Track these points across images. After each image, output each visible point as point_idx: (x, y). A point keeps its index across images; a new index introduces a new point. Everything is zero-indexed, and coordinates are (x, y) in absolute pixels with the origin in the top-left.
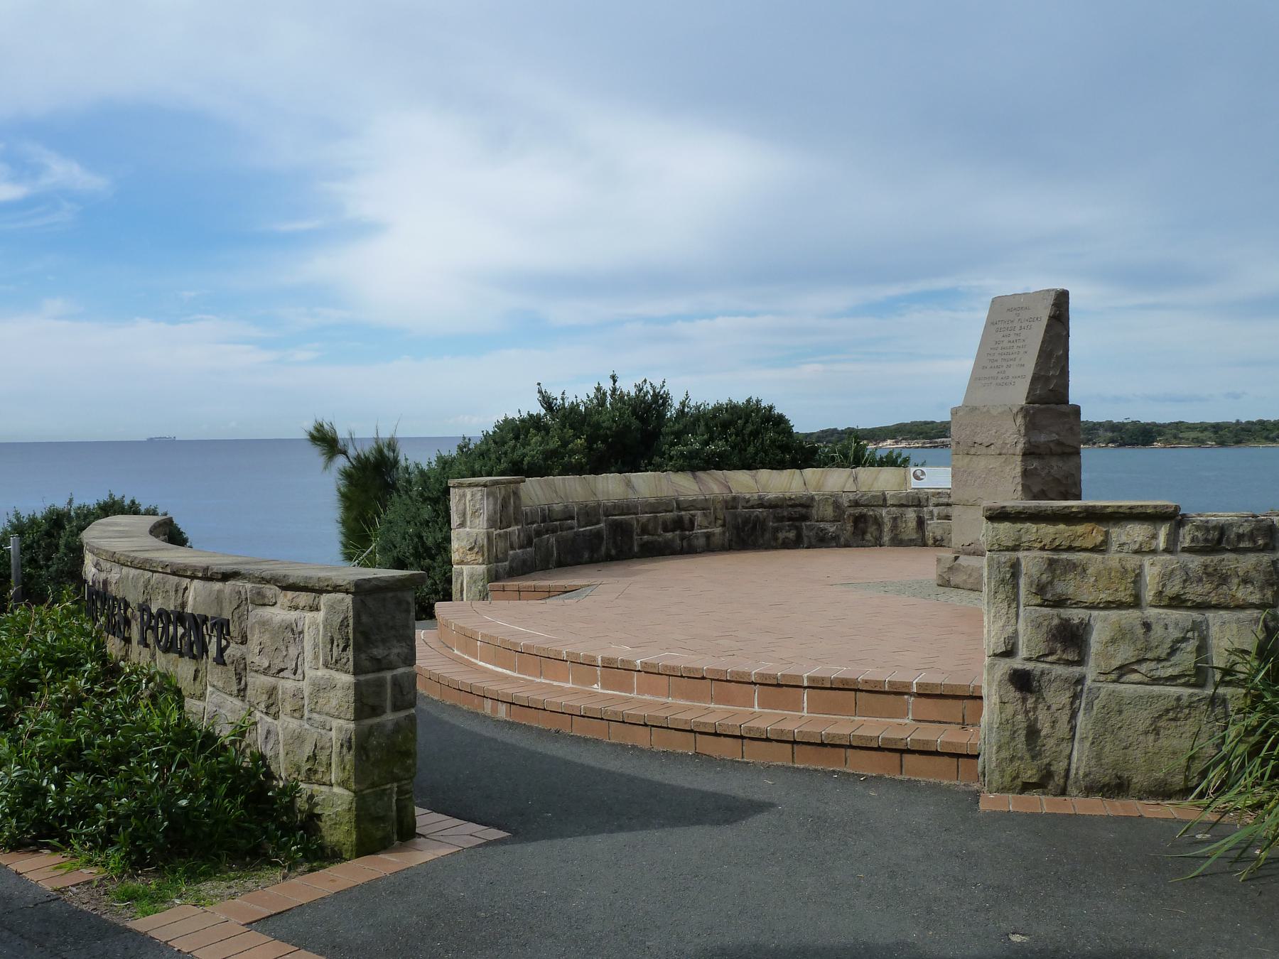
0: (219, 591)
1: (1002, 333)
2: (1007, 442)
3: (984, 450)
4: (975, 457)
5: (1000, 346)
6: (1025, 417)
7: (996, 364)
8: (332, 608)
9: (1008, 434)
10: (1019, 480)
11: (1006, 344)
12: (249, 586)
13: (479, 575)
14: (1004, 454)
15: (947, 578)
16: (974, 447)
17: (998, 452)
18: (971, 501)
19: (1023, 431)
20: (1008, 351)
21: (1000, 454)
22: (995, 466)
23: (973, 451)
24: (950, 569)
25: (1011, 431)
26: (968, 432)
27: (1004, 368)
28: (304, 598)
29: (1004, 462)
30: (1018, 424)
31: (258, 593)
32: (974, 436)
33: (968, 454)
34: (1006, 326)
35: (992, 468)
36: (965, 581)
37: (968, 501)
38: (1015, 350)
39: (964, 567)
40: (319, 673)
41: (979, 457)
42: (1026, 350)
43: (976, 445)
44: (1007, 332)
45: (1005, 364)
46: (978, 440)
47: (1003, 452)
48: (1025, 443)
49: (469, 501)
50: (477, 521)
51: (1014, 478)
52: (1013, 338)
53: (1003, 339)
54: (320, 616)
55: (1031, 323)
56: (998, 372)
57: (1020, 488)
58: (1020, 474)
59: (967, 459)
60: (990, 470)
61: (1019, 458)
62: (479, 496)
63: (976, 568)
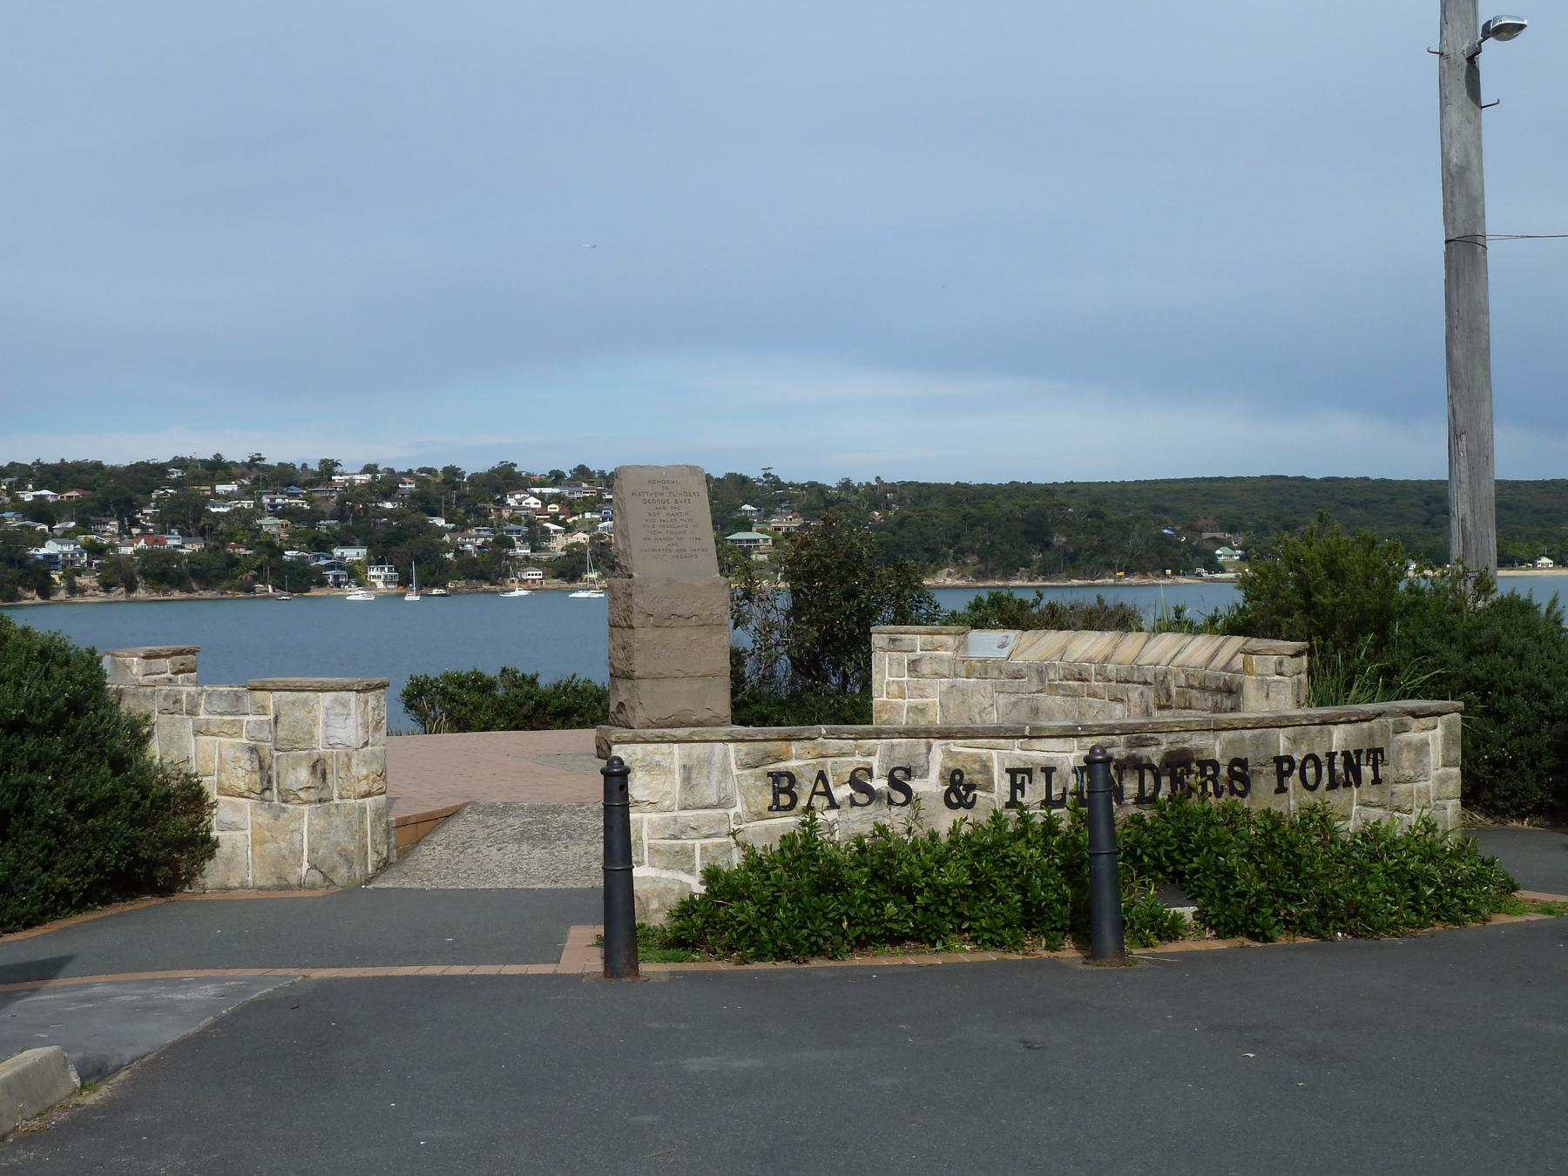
0: (1371, 729)
3: (681, 621)
4: (667, 630)
7: (659, 536)
8: (1448, 726)
11: (663, 516)
12: (1391, 720)
13: (383, 808)
14: (709, 625)
17: (701, 623)
23: (667, 623)
27: (675, 540)
28: (1429, 721)
31: (1402, 724)
40: (1439, 771)
41: (673, 630)
44: (661, 505)
46: (678, 613)
47: (708, 623)
49: (374, 709)
50: (377, 736)
53: (656, 511)
54: (1439, 732)
55: (689, 498)
59: (658, 632)
62: (372, 702)
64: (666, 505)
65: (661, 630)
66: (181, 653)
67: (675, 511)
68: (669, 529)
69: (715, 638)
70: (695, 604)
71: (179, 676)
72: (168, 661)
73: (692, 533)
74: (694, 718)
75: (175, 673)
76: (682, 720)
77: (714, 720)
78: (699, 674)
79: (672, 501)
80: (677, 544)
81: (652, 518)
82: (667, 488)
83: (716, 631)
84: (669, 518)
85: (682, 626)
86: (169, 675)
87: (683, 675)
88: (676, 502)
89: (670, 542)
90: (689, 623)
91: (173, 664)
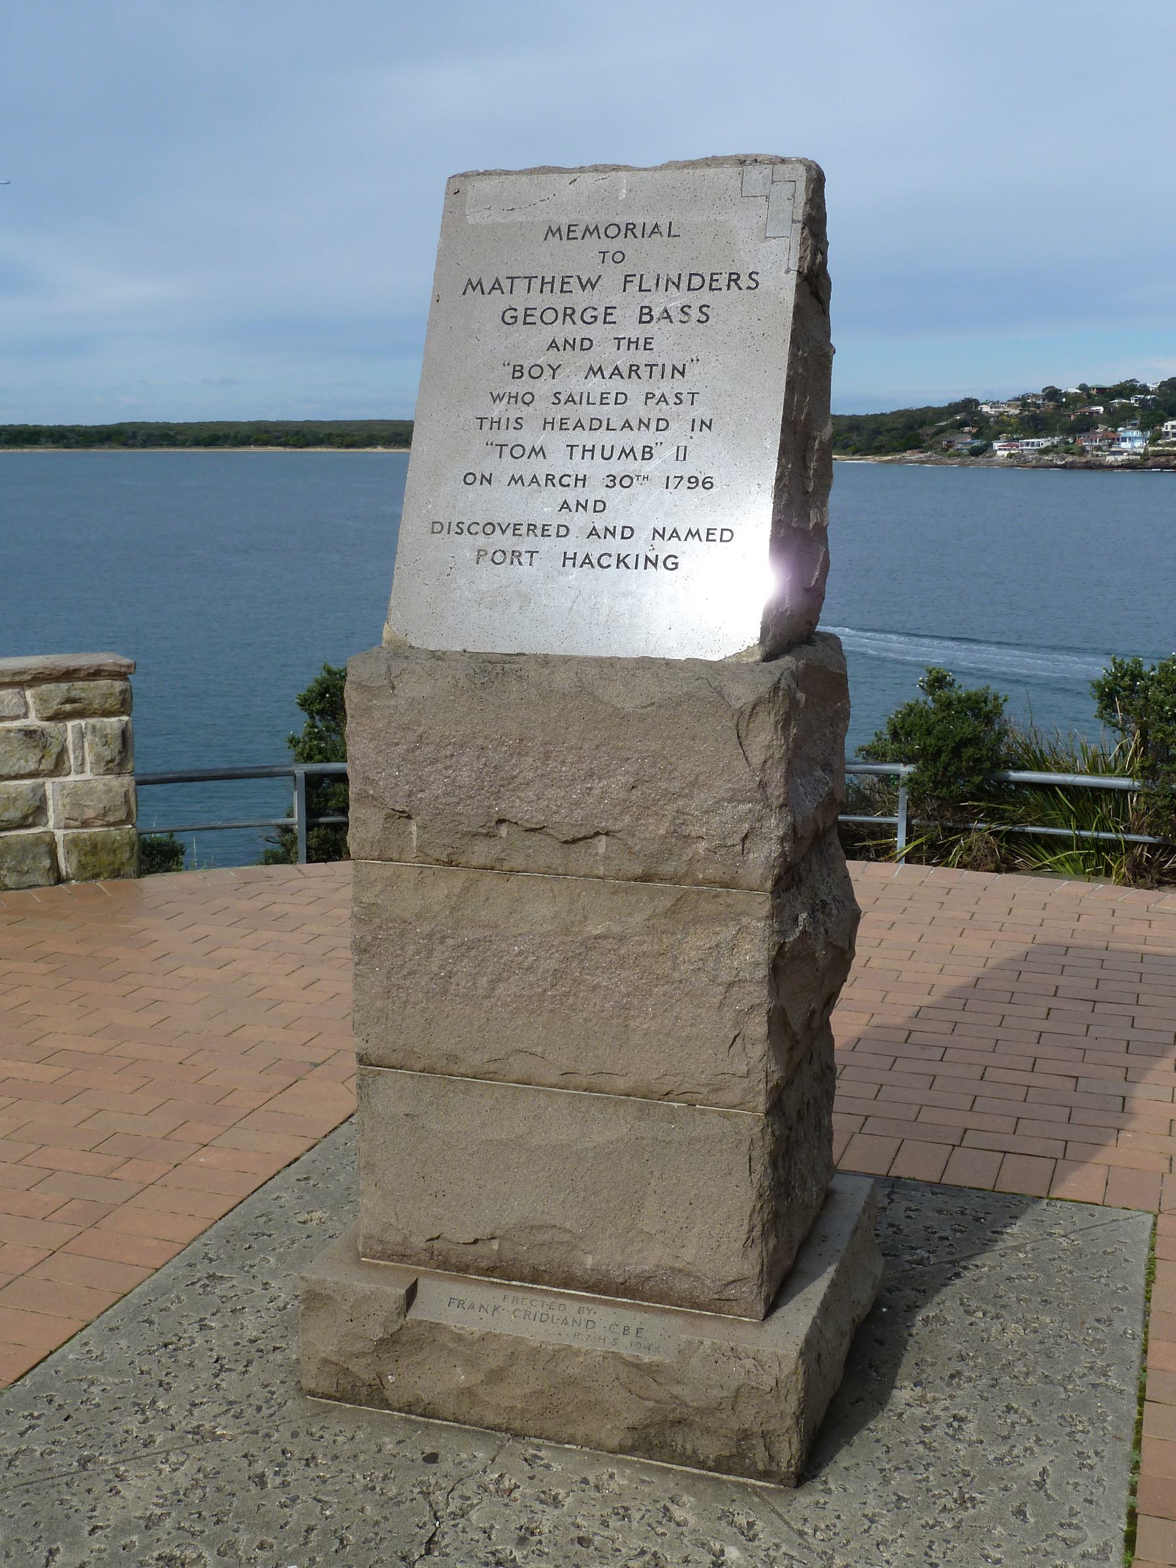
1: (547, 334)
2: (694, 830)
3: (547, 853)
4: (489, 881)
5: (544, 387)
6: (785, 723)
9: (703, 798)
10: (758, 995)
14: (675, 879)
15: (367, 1376)
16: (489, 835)
17: (638, 870)
18: (476, 1060)
19: (776, 791)
20: (604, 412)
21: (646, 878)
22: (616, 929)
23: (482, 852)
24: (390, 1343)
25: (722, 788)
26: (465, 776)
29: (670, 913)
30: (757, 758)
32: (497, 795)
33: (450, 863)
34: (560, 302)
35: (604, 937)
36: (468, 1392)
37: (453, 1058)
38: (636, 409)
39: (459, 1339)
41: (514, 882)
42: (701, 411)
43: (504, 830)
45: (597, 469)
46: (523, 808)
47: (668, 868)
48: (782, 840)
51: (730, 985)
52: (606, 354)
53: (553, 357)
55: (706, 296)
56: (565, 505)
57: (758, 1027)
58: (762, 972)
60: (591, 944)
61: (762, 905)
63: (535, 1352)
64: (597, 331)
65: (457, 881)
66: (69, 675)
67: (624, 359)
68: (583, 438)
69: (696, 943)
70: (599, 786)
71: (70, 724)
72: (28, 693)
73: (682, 454)
74: (589, 1261)
75: (58, 717)
76: (538, 1259)
77: (682, 1285)
78: (621, 1084)
79: (628, 307)
80: (600, 507)
81: (520, 387)
82: (620, 257)
83: (706, 907)
84: (596, 385)
85: (550, 873)
86: (33, 721)
87: (553, 1078)
88: (645, 315)
89: (571, 496)
90: (579, 858)
91: (42, 700)
